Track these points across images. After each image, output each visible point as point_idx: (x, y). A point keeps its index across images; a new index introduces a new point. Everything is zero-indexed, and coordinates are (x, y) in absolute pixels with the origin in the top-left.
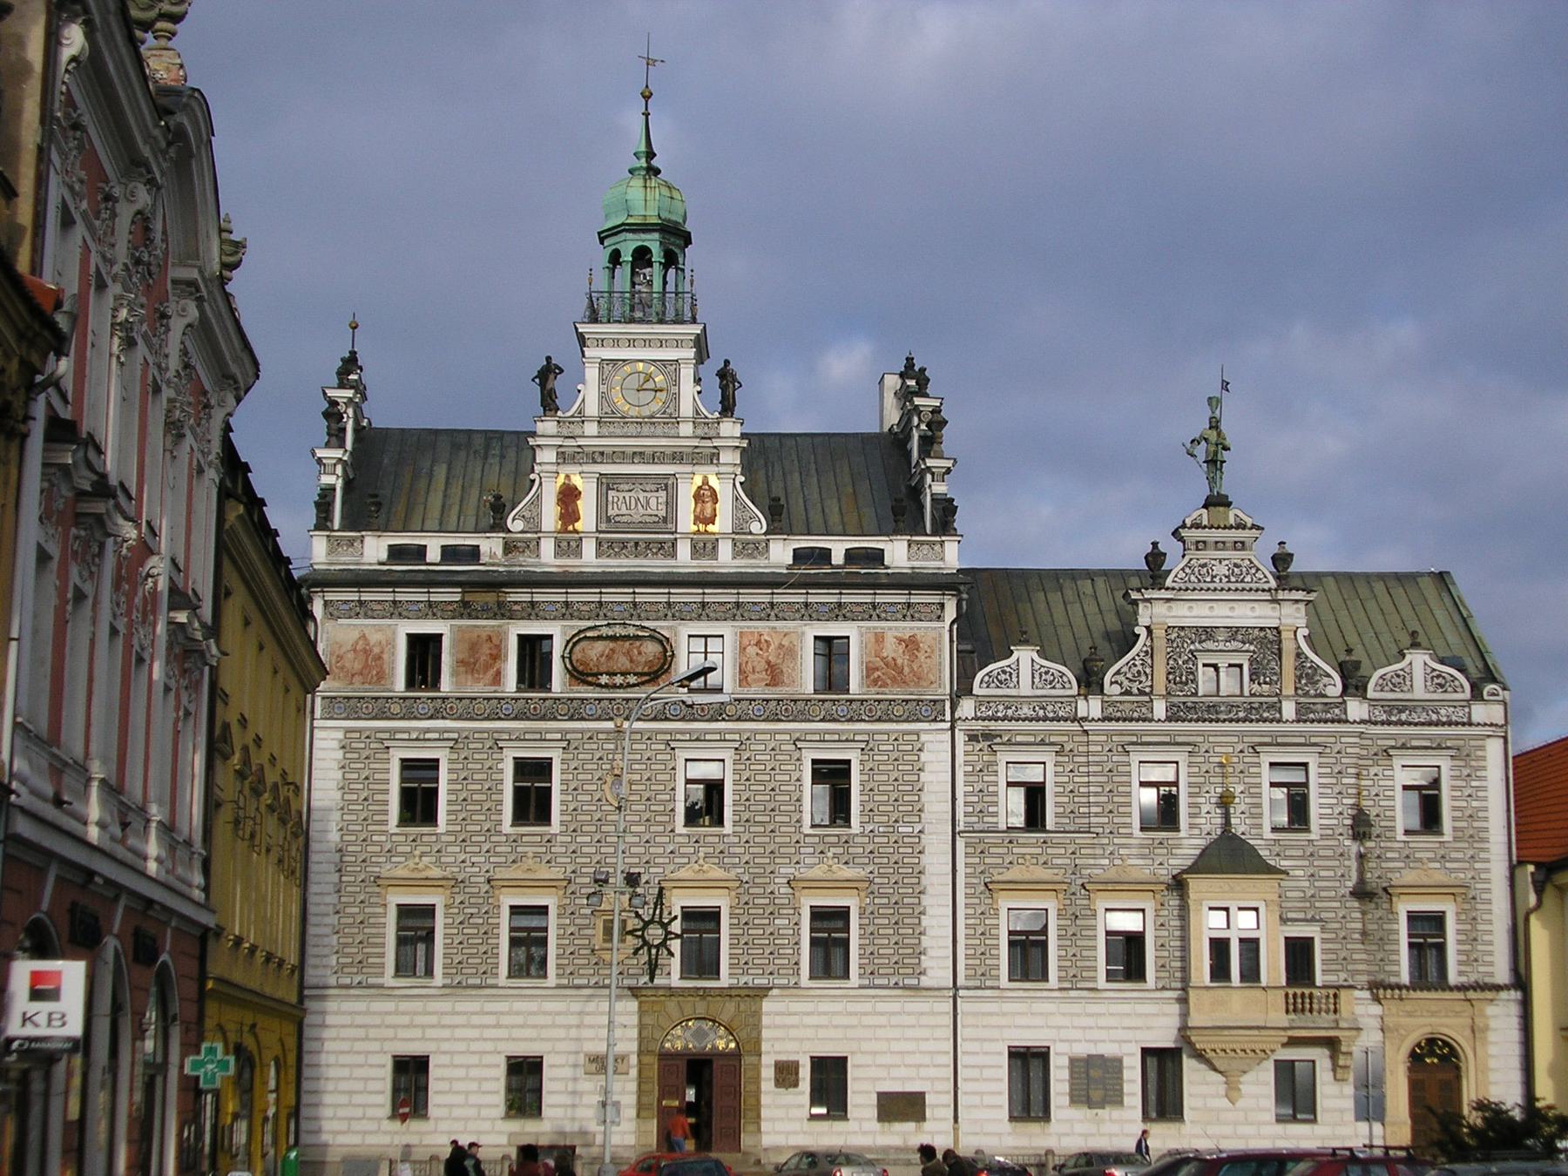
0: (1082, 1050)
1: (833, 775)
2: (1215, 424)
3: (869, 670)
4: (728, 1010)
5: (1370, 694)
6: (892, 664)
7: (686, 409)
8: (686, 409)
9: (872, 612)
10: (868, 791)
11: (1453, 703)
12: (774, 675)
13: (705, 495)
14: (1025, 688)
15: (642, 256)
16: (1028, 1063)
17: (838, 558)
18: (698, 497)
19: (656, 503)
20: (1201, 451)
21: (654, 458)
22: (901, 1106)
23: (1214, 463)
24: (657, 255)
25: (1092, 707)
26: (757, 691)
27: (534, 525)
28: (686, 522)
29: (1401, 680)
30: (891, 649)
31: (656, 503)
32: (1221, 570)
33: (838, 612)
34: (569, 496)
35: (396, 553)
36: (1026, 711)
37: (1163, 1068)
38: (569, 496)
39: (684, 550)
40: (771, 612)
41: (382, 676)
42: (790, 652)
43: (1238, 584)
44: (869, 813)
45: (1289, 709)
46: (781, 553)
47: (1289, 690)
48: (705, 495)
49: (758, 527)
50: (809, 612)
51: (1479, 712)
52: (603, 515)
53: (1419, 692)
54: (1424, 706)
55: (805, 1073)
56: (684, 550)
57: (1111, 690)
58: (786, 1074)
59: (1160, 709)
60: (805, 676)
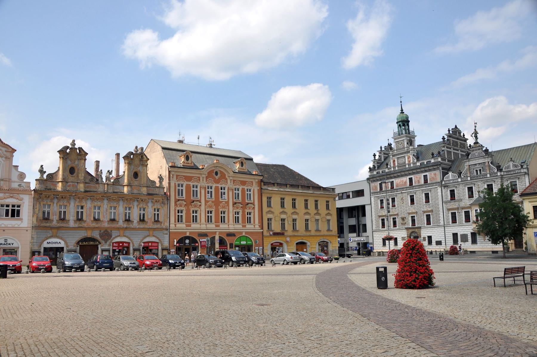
0: (462, 233)
1: (427, 196)
2: (475, 130)
3: (430, 179)
4: (416, 230)
5: (504, 170)
6: (433, 178)
7: (406, 146)
8: (406, 146)
9: (430, 170)
10: (431, 197)
11: (518, 170)
12: (419, 182)
13: (409, 158)
14: (451, 178)
15: (400, 125)
16: (455, 235)
17: (425, 163)
18: (408, 158)
19: (404, 160)
20: (473, 135)
21: (401, 154)
22: (439, 243)
23: (476, 137)
24: (401, 125)
25: (460, 180)
26: (417, 184)
27: (390, 166)
28: (407, 162)
29: (508, 167)
30: (433, 175)
31: (404, 160)
32: (477, 154)
33: (426, 171)
34: (394, 161)
35: (377, 173)
36: (451, 182)
37: (473, 235)
38: (394, 161)
39: (407, 166)
40: (418, 173)
41: (377, 189)
42: (420, 178)
43: (480, 157)
44: (432, 200)
45: (488, 176)
46: (418, 164)
47: (488, 172)
48: (409, 158)
49: (415, 161)
50: (422, 172)
51: (522, 171)
52: (398, 163)
53: (512, 168)
54: (513, 171)
55: (427, 238)
56: (407, 166)
57: (462, 176)
58: (424, 238)
59: (469, 179)
60: (422, 182)
